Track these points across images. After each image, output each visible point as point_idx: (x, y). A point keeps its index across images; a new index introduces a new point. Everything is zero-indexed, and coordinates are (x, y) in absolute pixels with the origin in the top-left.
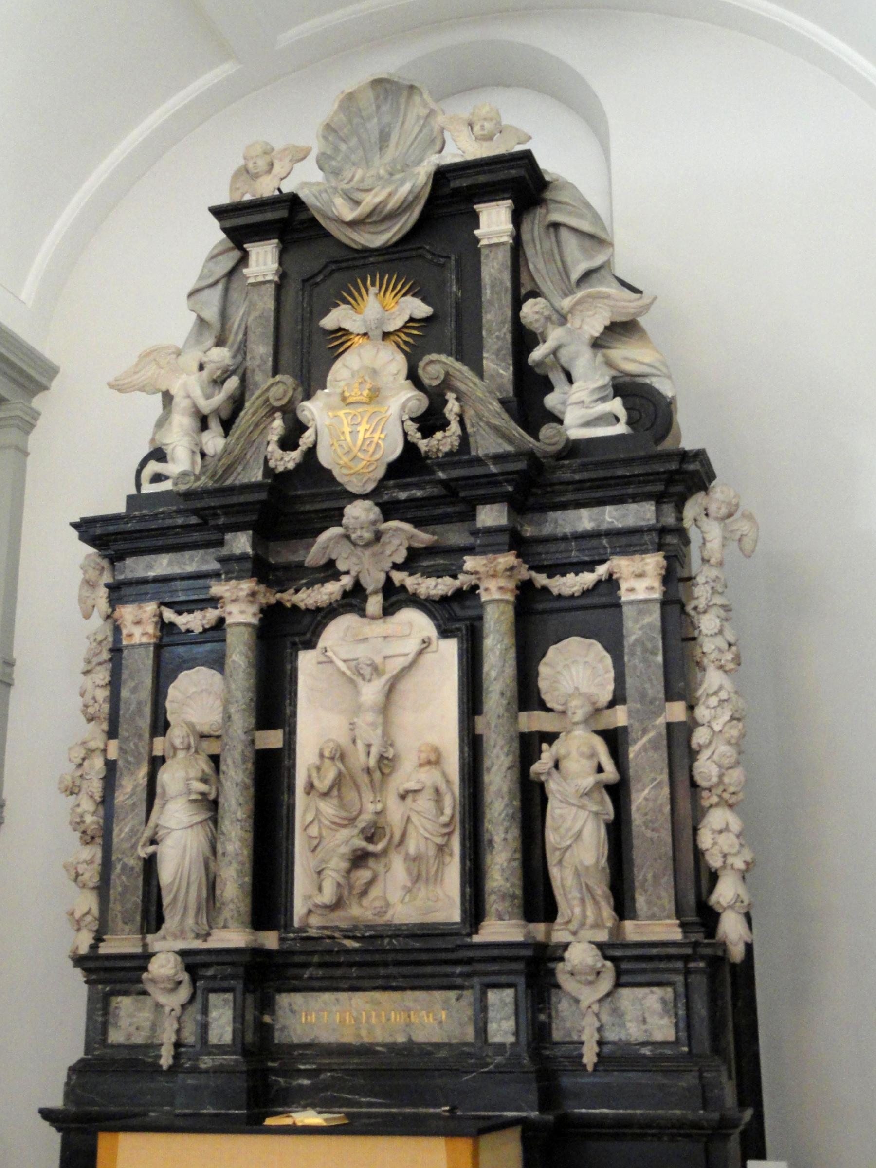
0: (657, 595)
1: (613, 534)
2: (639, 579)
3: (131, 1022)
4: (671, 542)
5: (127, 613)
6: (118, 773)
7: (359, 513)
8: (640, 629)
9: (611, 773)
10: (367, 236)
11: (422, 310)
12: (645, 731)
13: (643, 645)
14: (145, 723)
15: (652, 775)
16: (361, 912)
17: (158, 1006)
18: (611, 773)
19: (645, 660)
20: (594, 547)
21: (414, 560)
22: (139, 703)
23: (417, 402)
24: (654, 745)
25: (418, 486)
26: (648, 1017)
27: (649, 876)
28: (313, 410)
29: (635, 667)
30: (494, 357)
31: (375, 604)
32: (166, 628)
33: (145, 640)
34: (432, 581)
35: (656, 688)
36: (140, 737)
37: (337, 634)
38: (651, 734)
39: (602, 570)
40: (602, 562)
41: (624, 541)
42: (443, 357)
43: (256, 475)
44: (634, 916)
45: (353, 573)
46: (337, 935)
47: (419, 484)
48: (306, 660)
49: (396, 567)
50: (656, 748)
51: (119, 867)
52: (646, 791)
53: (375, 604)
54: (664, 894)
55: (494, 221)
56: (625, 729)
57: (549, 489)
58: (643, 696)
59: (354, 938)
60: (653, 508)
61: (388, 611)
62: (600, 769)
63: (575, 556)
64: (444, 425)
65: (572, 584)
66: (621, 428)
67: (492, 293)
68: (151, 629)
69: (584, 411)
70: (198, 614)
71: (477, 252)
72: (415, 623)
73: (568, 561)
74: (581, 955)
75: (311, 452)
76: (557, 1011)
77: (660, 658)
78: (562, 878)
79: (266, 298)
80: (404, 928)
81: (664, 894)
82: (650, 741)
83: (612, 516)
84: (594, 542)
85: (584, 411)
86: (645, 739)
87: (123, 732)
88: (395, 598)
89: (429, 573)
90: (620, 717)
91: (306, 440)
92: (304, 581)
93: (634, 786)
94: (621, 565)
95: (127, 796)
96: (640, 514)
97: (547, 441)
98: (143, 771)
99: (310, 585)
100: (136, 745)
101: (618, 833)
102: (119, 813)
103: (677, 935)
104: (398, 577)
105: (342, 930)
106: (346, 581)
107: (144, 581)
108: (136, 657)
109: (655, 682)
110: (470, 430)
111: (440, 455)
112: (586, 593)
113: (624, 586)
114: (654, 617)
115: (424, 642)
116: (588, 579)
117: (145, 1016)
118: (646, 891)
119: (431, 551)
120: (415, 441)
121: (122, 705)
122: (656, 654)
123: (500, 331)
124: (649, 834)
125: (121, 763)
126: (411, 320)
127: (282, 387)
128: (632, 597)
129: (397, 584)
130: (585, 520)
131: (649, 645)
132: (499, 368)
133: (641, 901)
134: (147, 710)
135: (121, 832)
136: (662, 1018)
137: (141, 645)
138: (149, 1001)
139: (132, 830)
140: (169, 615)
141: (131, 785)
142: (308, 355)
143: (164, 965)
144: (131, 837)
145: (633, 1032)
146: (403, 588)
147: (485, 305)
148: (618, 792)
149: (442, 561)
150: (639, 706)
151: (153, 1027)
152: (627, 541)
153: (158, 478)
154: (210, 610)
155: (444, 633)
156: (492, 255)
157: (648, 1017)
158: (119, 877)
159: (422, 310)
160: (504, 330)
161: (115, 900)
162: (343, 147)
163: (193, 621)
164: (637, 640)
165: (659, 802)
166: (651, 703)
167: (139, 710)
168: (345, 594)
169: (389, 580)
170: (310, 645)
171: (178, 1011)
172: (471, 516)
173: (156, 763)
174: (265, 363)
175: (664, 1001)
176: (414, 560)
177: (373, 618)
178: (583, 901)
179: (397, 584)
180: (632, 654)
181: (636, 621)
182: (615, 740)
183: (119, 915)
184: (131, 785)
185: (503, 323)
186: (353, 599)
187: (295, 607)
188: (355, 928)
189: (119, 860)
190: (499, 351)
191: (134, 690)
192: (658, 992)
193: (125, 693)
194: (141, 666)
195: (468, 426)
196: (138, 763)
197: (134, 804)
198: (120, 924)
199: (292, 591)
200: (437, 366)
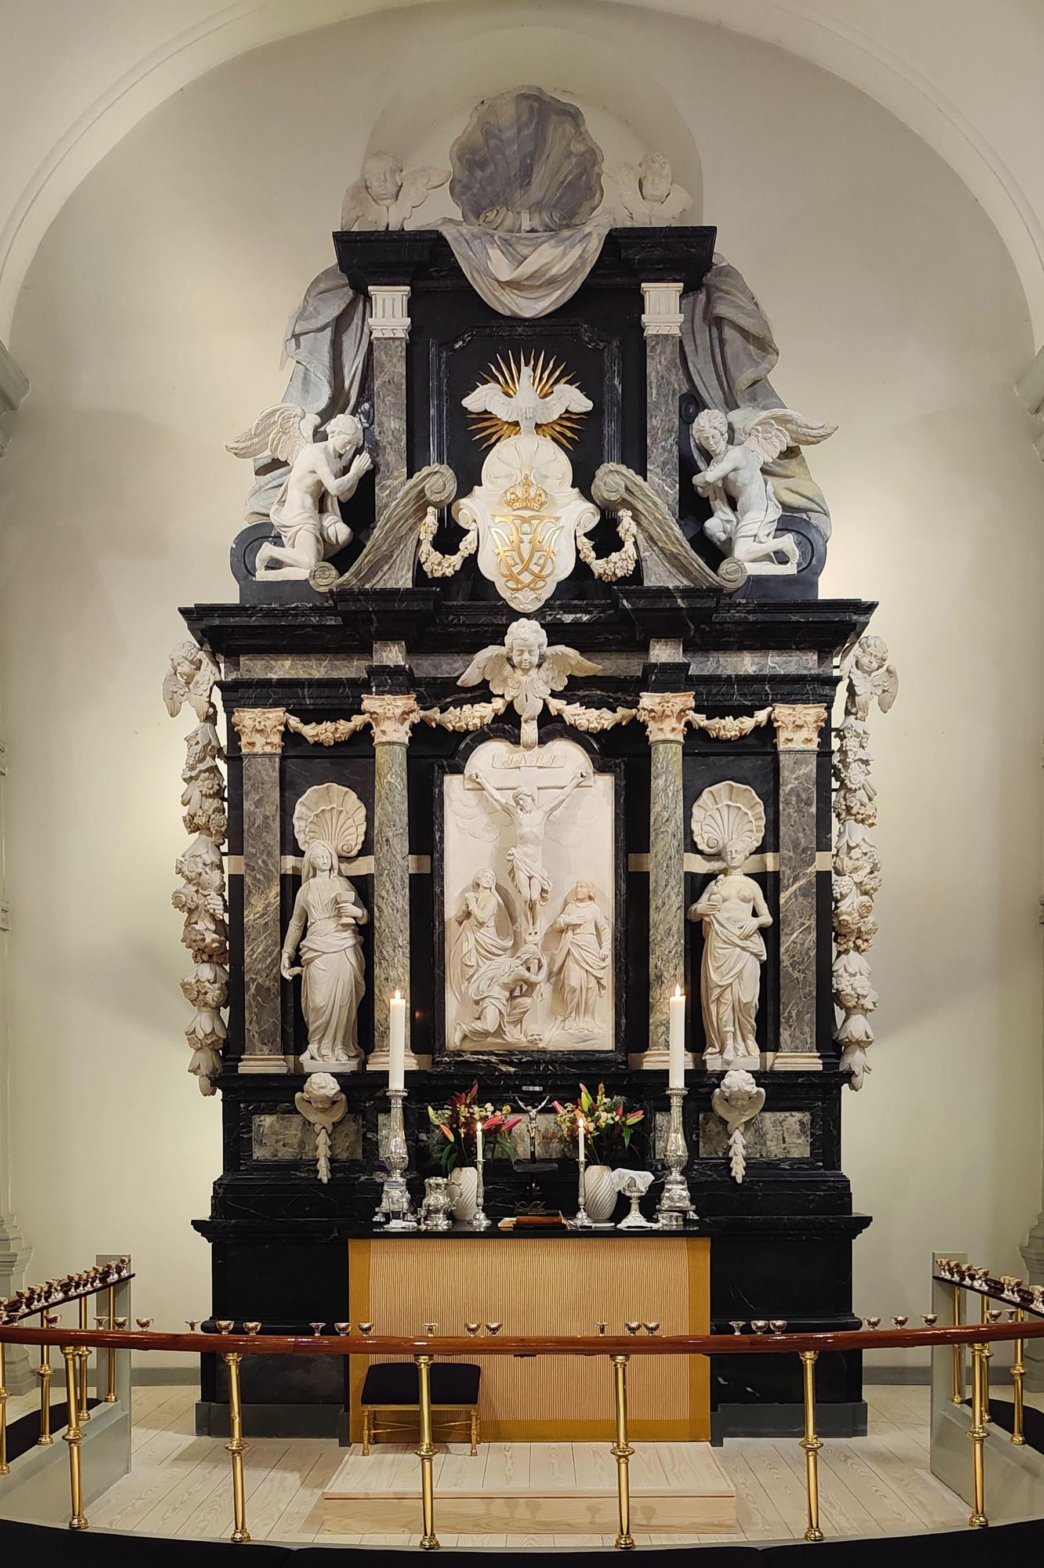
0: (814, 746)
1: (776, 680)
2: (796, 726)
3: (272, 1136)
5: (248, 717)
6: (246, 892)
8: (796, 779)
9: (766, 919)
10: (519, 300)
11: (582, 404)
12: (796, 879)
13: (798, 796)
14: (274, 839)
15: (800, 920)
16: (516, 1037)
17: (307, 1124)
18: (766, 919)
19: (799, 811)
21: (576, 689)
22: (266, 817)
23: (588, 517)
24: (804, 892)
25: (587, 612)
26: (788, 1135)
27: (794, 1013)
28: (470, 511)
29: (789, 815)
30: (659, 470)
31: (529, 731)
32: (290, 737)
33: (268, 749)
34: (593, 713)
35: (808, 838)
36: (270, 854)
37: (488, 758)
38: (802, 882)
39: (761, 716)
40: (763, 708)
41: (787, 689)
42: (623, 468)
43: (404, 580)
44: (776, 1049)
45: (508, 698)
46: (494, 1059)
47: (598, 613)
48: (453, 785)
49: (554, 694)
50: (805, 896)
51: (253, 988)
52: (795, 935)
53: (529, 731)
54: (807, 1029)
55: (662, 307)
56: (776, 874)
57: (718, 627)
58: (796, 845)
59: (511, 1063)
60: (816, 657)
61: (542, 741)
62: (755, 914)
63: (737, 699)
64: (619, 545)
65: (730, 727)
66: (790, 569)
67: (658, 394)
68: (276, 739)
69: (754, 544)
70: (328, 725)
71: (644, 344)
72: (569, 756)
73: (728, 703)
75: (471, 561)
76: (704, 1132)
77: (813, 809)
78: (721, 1015)
79: (395, 360)
80: (560, 1055)
81: (807, 1029)
82: (800, 888)
84: (756, 687)
85: (754, 544)
86: (795, 886)
87: (248, 849)
88: (552, 726)
89: (588, 704)
90: (771, 862)
91: (466, 546)
92: (448, 700)
93: (785, 930)
94: (783, 712)
95: (257, 916)
96: (802, 663)
97: (728, 577)
98: (275, 890)
99: (459, 704)
100: (263, 861)
101: (770, 973)
102: (250, 933)
103: (817, 1065)
104: (556, 705)
105: (496, 1055)
106: (498, 704)
107: (267, 683)
108: (260, 768)
109: (809, 833)
110: (642, 555)
111: (614, 580)
112: (742, 737)
113: (782, 736)
114: (810, 768)
115: (582, 776)
116: (747, 724)
117: (293, 1131)
118: (790, 1026)
119: (591, 681)
120: (588, 560)
121: (246, 820)
122: (810, 805)
123: (666, 440)
124: (796, 974)
125: (248, 880)
126: (567, 411)
127: (438, 478)
128: (790, 745)
129: (554, 713)
130: (747, 664)
131: (804, 796)
133: (785, 1035)
134: (276, 826)
135: (254, 951)
136: (799, 1138)
137: (264, 755)
138: (296, 1119)
139: (265, 951)
140: (294, 722)
141: (262, 904)
144: (266, 958)
145: (774, 1149)
146: (560, 717)
147: (650, 406)
148: (771, 935)
149: (599, 692)
150: (791, 854)
151: (302, 1144)
153: (275, 564)
154: (342, 721)
155: (601, 768)
156: (659, 349)
157: (788, 1135)
158: (254, 997)
159: (582, 404)
160: (670, 441)
161: (251, 1023)
162: (479, 174)
163: (323, 732)
164: (792, 789)
165: (806, 945)
166: (804, 851)
167: (266, 825)
168: (497, 718)
169: (546, 706)
170: (459, 770)
171: (330, 1129)
172: (646, 650)
173: (291, 884)
174: (398, 440)
175: (802, 1123)
176: (576, 689)
177: (529, 747)
178: (734, 1033)
179: (554, 713)
180: (788, 803)
181: (793, 771)
182: (769, 884)
183: (256, 1036)
184: (262, 904)
185: (670, 431)
186: (506, 726)
187: (440, 727)
188: (511, 1053)
189: (254, 980)
190: (665, 464)
191: (258, 804)
192: (798, 1115)
193: (248, 805)
194: (266, 778)
195: (642, 550)
196: (269, 880)
197: (266, 924)
198: (258, 1045)
199: (436, 709)
200: (613, 478)
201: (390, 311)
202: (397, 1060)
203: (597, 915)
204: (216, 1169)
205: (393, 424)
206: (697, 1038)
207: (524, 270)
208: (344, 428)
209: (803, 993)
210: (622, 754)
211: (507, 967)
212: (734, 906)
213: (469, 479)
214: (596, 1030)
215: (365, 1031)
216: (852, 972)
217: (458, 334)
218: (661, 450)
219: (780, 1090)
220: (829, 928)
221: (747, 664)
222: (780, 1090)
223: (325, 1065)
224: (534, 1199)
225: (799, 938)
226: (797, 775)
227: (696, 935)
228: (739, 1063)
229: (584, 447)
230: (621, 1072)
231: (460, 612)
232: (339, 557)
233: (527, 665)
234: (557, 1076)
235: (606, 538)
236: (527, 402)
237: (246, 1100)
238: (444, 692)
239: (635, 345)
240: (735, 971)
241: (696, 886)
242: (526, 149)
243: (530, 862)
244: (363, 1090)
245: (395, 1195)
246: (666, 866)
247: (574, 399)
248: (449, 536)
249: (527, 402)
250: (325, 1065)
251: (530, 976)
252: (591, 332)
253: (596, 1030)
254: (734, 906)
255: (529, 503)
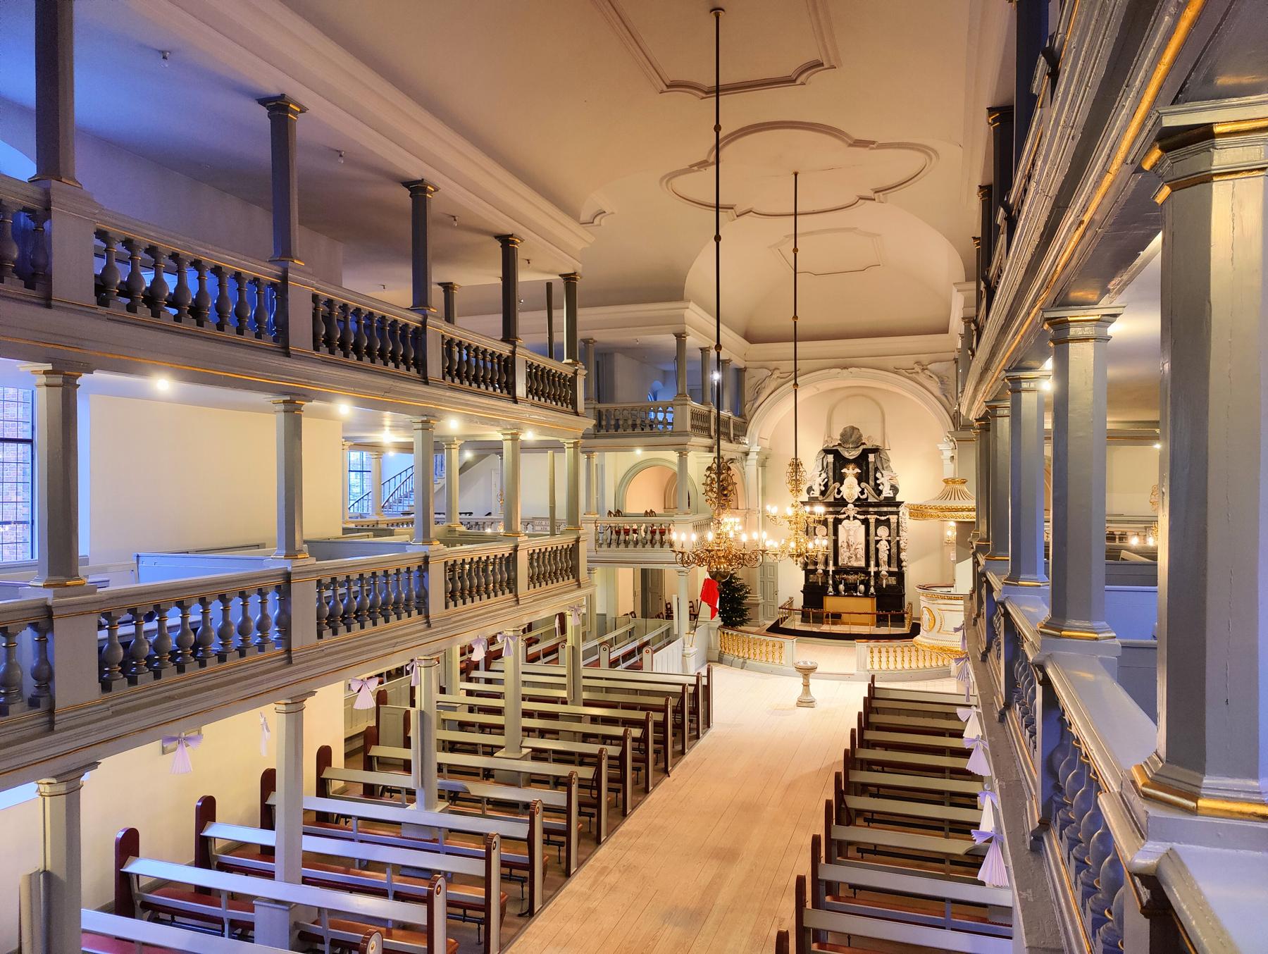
2: (893, 518)
4: (897, 513)
7: (850, 506)
20: (886, 513)
26: (893, 581)
37: (845, 522)
47: (861, 503)
55: (871, 457)
69: (887, 492)
72: (858, 523)
74: (884, 573)
78: (881, 562)
83: (890, 509)
85: (887, 492)
88: (855, 518)
96: (894, 509)
101: (889, 556)
130: (885, 509)
132: (872, 483)
142: (840, 478)
143: (820, 571)
152: (892, 513)
157: (893, 581)
182: (889, 542)
186: (848, 518)
200: (863, 485)
201: (830, 458)
202: (831, 568)
203: (862, 546)
204: (803, 582)
205: (831, 474)
206: (877, 564)
207: (851, 454)
208: (824, 475)
209: (896, 558)
210: (865, 522)
211: (848, 554)
212: (883, 546)
213: (842, 484)
214: (862, 564)
215: (826, 563)
216: (903, 556)
217: (840, 461)
218: (871, 478)
219: (891, 574)
220: (899, 550)
221: (885, 509)
222: (891, 574)
223: (820, 568)
224: (851, 589)
225: (894, 550)
226: (893, 526)
227: (877, 550)
228: (884, 569)
229: (861, 478)
230: (864, 570)
231: (841, 503)
232: (823, 493)
233: (851, 510)
234: (856, 570)
235: (862, 493)
236: (851, 472)
237: (808, 573)
238: (838, 513)
239: (868, 463)
240: (883, 556)
241: (877, 542)
242: (851, 436)
243: (852, 540)
244: (826, 572)
245: (831, 589)
246: (872, 538)
247: (858, 470)
248: (839, 492)
249: (851, 472)
250: (820, 568)
251: (852, 554)
252: (861, 461)
253: (862, 564)
254: (883, 546)
255: (851, 488)
